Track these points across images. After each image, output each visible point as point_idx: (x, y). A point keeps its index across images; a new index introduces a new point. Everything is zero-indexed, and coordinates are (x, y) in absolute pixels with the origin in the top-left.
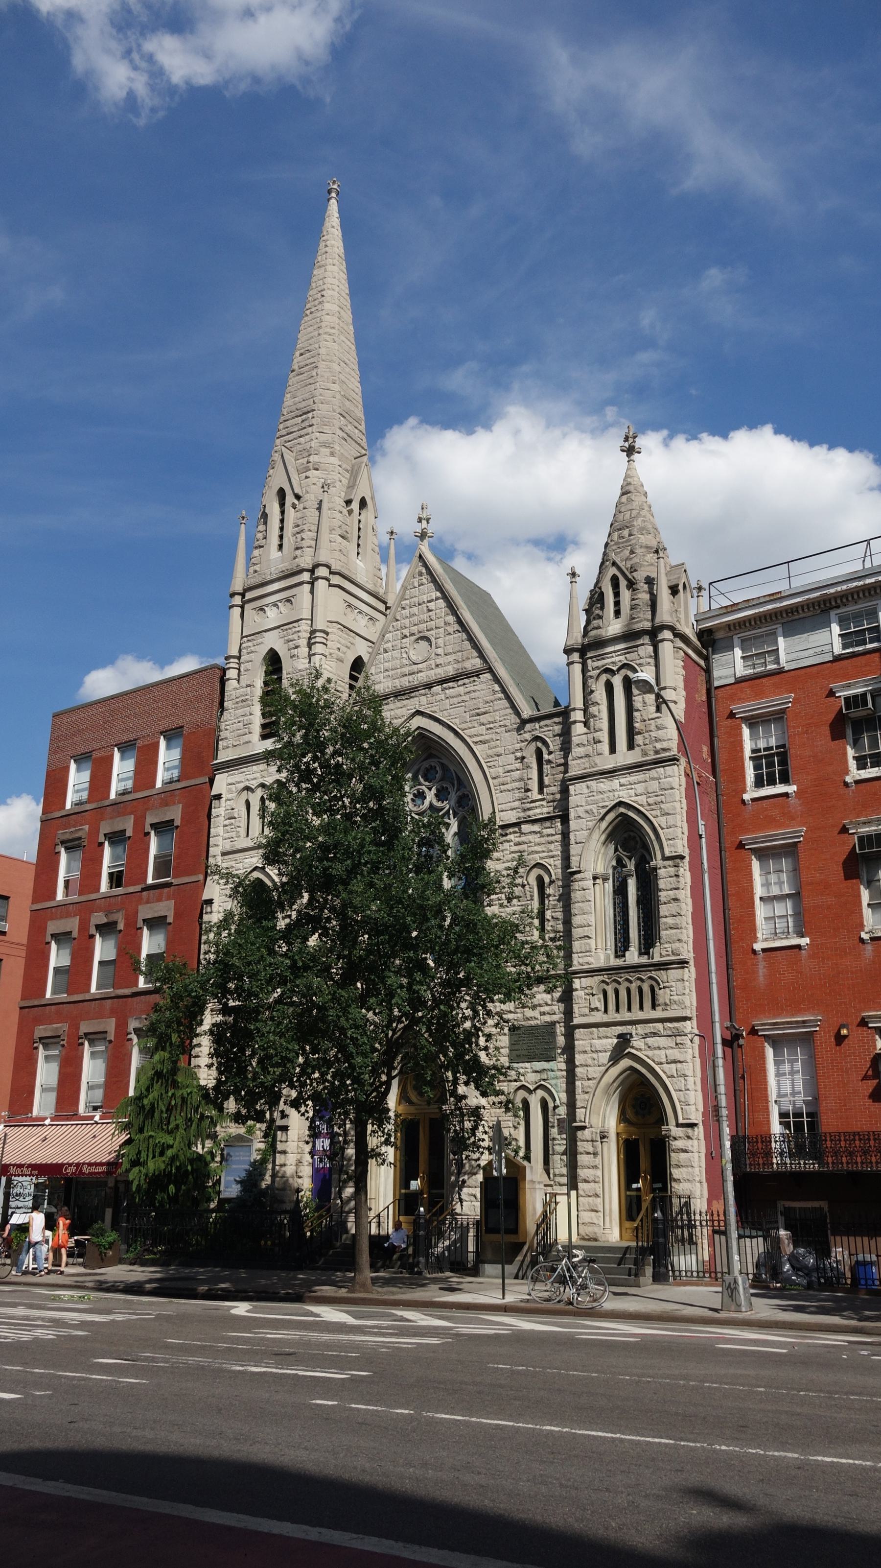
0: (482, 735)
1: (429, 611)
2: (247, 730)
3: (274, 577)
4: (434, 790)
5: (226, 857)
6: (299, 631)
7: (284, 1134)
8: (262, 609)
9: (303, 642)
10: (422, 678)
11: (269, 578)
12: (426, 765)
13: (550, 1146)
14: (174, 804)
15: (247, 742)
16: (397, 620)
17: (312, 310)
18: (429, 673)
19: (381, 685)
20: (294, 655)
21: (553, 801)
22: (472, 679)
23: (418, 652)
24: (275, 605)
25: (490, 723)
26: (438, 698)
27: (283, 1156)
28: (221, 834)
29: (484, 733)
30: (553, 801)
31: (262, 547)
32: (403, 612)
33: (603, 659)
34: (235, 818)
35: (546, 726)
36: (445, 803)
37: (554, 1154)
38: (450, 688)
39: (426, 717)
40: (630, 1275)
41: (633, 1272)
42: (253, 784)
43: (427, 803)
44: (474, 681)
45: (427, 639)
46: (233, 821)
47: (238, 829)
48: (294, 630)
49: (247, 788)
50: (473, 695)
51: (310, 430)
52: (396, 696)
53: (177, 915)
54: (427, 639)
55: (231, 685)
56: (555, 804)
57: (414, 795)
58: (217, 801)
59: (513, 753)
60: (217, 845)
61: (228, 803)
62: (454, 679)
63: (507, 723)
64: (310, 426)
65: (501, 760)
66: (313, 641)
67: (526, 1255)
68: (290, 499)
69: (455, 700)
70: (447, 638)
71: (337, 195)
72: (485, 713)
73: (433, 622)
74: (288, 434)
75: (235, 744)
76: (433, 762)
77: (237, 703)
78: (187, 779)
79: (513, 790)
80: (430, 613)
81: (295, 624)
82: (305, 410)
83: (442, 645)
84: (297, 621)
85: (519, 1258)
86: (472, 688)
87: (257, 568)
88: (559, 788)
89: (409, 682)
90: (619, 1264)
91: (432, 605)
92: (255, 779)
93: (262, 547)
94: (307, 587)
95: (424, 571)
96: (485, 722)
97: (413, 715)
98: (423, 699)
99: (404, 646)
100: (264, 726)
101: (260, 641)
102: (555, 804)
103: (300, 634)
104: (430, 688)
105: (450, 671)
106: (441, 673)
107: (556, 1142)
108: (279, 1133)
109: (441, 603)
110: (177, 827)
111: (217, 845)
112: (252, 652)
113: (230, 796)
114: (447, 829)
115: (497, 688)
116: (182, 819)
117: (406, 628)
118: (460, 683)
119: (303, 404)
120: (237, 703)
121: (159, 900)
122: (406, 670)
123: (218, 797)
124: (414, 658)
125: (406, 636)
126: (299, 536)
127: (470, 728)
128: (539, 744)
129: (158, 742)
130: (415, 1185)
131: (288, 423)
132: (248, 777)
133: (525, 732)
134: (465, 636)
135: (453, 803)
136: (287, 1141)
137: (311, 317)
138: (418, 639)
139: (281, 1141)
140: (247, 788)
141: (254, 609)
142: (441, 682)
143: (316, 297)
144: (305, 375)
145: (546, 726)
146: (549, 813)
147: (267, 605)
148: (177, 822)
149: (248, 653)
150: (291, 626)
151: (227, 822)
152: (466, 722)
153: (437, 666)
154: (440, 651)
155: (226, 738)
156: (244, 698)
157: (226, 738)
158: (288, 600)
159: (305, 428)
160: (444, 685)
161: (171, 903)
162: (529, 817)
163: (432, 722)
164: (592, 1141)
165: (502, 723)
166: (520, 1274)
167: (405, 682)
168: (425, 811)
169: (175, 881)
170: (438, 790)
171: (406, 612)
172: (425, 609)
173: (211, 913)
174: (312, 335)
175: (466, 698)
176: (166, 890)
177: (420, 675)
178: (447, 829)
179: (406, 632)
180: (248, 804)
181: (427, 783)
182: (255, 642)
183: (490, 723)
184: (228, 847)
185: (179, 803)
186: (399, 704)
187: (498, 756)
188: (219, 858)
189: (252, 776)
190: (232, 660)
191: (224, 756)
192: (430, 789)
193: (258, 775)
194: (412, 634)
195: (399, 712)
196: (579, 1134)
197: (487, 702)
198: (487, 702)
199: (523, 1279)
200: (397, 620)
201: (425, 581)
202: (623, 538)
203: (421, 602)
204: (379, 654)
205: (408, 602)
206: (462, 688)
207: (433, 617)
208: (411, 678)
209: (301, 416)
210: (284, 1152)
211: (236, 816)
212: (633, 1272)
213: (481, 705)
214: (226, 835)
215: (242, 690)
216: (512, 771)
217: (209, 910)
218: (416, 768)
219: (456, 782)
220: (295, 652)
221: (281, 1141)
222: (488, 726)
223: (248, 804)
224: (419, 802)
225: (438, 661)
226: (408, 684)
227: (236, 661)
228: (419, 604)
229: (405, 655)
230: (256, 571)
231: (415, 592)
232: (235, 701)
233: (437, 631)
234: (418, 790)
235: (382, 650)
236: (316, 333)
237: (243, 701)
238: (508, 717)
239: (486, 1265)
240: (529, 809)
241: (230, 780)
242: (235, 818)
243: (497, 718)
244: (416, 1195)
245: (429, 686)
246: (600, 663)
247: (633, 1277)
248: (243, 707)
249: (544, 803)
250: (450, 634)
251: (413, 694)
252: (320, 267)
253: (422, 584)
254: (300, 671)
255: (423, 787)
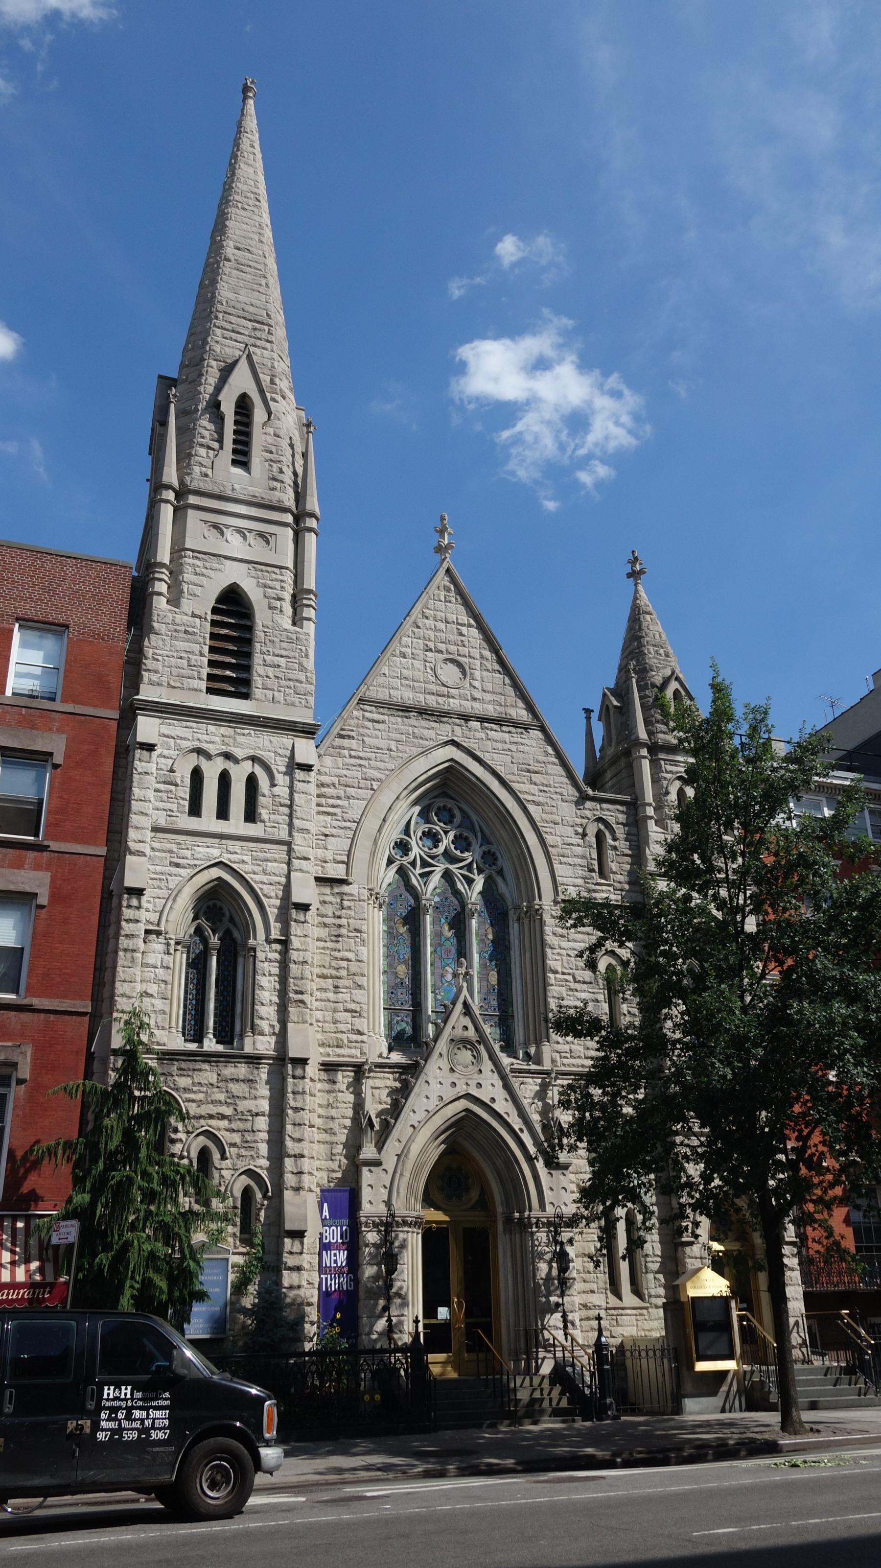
0: (534, 795)
1: (461, 634)
2: (195, 674)
3: (242, 497)
4: (451, 835)
5: (159, 835)
6: (282, 581)
7: (297, 1243)
8: (216, 526)
9: (288, 597)
10: (454, 704)
11: (229, 493)
12: (440, 802)
13: (643, 1263)
14: (50, 729)
15: (196, 690)
16: (418, 627)
17: (246, 207)
18: (463, 702)
19: (399, 692)
20: (275, 608)
21: (622, 890)
22: (519, 730)
23: (449, 674)
24: (239, 531)
25: (543, 785)
26: (478, 735)
27: (295, 1275)
28: (152, 799)
29: (537, 793)
30: (622, 890)
31: (213, 449)
32: (426, 621)
33: (676, 765)
34: (177, 785)
35: (608, 810)
36: (466, 854)
37: (647, 1272)
38: (492, 730)
39: (463, 751)
40: (859, 1395)
41: (863, 1391)
42: (212, 749)
43: (441, 849)
44: (522, 733)
45: (459, 665)
46: (173, 788)
47: (181, 802)
48: (274, 576)
49: (199, 751)
50: (521, 747)
51: (268, 345)
52: (421, 713)
53: (53, 896)
54: (459, 665)
55: (160, 604)
56: (624, 893)
57: (424, 833)
58: (145, 752)
59: (572, 826)
60: (146, 815)
61: (163, 760)
62: (499, 721)
63: (564, 792)
64: (268, 341)
65: (559, 829)
66: (299, 603)
67: (731, 1384)
68: (259, 415)
69: (500, 746)
70: (485, 673)
71: (254, 96)
72: (536, 772)
73: (466, 650)
74: (233, 331)
75: (173, 684)
76: (450, 804)
77: (176, 631)
78: (76, 702)
79: (575, 865)
80: (463, 638)
81: (277, 570)
82: (259, 318)
83: (479, 678)
84: (281, 568)
85: (724, 1388)
86: (520, 740)
87: (209, 472)
88: (627, 879)
89: (439, 704)
90: (835, 1385)
91: (464, 630)
92: (213, 743)
93: (213, 449)
94: (290, 533)
95: (452, 587)
96: (538, 782)
97: (446, 743)
98: (458, 730)
99: (428, 659)
100: (210, 677)
101: (215, 565)
102: (624, 893)
103: (283, 584)
104: (467, 720)
105: (491, 710)
106: (478, 708)
107: (649, 1259)
108: (287, 1241)
109: (475, 632)
110: (56, 766)
111: (146, 815)
112: (203, 575)
113: (166, 752)
114: (470, 886)
115: (550, 750)
116: (67, 756)
117: (430, 640)
118: (505, 728)
119: (251, 309)
120: (176, 631)
121: (18, 865)
122: (433, 688)
123: (150, 747)
124: (443, 679)
125: (431, 650)
126: (274, 465)
127: (518, 782)
128: (602, 827)
129: (12, 630)
130: (443, 1313)
131: (233, 319)
132: (200, 736)
133: (584, 809)
134: (507, 681)
135: (478, 857)
136: (301, 1253)
137: (242, 212)
138: (446, 660)
139: (291, 1253)
140: (199, 751)
141: (206, 522)
142: (482, 719)
143: (249, 195)
144: (249, 276)
145: (608, 810)
146: (617, 901)
147: (228, 526)
148: (58, 759)
149: (196, 574)
150: (269, 569)
151: (162, 787)
152: (513, 774)
153: (475, 699)
154: (476, 684)
155: (156, 672)
156: (191, 630)
157: (156, 672)
158: (261, 535)
159: (260, 339)
160: (486, 724)
161: (45, 877)
162: (595, 899)
163: (470, 760)
164: (701, 1258)
165: (558, 790)
166: (727, 1406)
167: (432, 701)
168: (438, 856)
169: (54, 846)
170: (455, 836)
171: (430, 623)
172: (455, 630)
173: (139, 908)
174: (251, 235)
175: (513, 748)
176: (31, 855)
177: (451, 700)
178: (470, 886)
179: (431, 645)
180: (197, 775)
181: (442, 824)
182: (207, 564)
183: (543, 785)
184: (162, 822)
185: (60, 731)
186: (424, 723)
187: (555, 824)
188: (149, 834)
189: (206, 737)
190: (164, 570)
191: (147, 693)
192: (446, 833)
193: (217, 739)
194: (441, 652)
195: (426, 732)
196: (688, 1250)
197: (538, 762)
198: (538, 762)
199: (730, 1412)
200: (418, 627)
201: (453, 600)
202: (661, 655)
203: (450, 620)
204: (394, 655)
205: (432, 612)
206: (507, 735)
207: (466, 643)
208: (440, 700)
209: (250, 320)
210: (299, 1268)
211: (179, 782)
212: (863, 1391)
213: (531, 762)
214: (161, 805)
215: (186, 617)
216: (572, 845)
217: (134, 902)
218: (426, 802)
219: (479, 834)
220: (278, 604)
221: (291, 1253)
222: (542, 788)
223: (197, 775)
224: (429, 843)
225: (477, 695)
226: (435, 705)
227: (167, 573)
228: (447, 622)
229: (429, 670)
230: (206, 475)
231: (441, 606)
232: (172, 627)
233: (472, 661)
234: (430, 829)
235: (398, 652)
236: (256, 237)
237: (186, 632)
238: (564, 786)
239: (686, 1400)
240: (594, 891)
241: (165, 730)
242: (177, 785)
243: (552, 782)
244: (446, 1325)
245: (466, 718)
246: (674, 769)
247: (862, 1397)
248: (188, 641)
249: (611, 889)
250: (488, 670)
251: (445, 719)
252: (248, 165)
253: (450, 602)
254: (286, 630)
255: (437, 828)
